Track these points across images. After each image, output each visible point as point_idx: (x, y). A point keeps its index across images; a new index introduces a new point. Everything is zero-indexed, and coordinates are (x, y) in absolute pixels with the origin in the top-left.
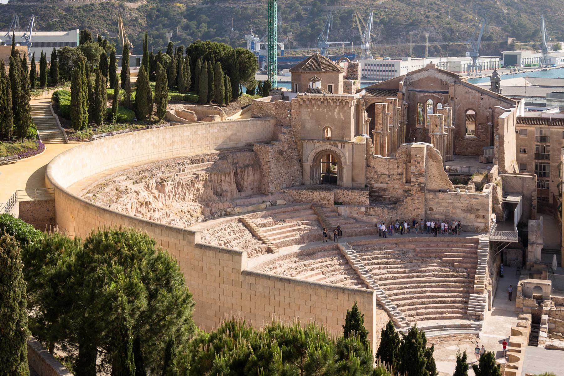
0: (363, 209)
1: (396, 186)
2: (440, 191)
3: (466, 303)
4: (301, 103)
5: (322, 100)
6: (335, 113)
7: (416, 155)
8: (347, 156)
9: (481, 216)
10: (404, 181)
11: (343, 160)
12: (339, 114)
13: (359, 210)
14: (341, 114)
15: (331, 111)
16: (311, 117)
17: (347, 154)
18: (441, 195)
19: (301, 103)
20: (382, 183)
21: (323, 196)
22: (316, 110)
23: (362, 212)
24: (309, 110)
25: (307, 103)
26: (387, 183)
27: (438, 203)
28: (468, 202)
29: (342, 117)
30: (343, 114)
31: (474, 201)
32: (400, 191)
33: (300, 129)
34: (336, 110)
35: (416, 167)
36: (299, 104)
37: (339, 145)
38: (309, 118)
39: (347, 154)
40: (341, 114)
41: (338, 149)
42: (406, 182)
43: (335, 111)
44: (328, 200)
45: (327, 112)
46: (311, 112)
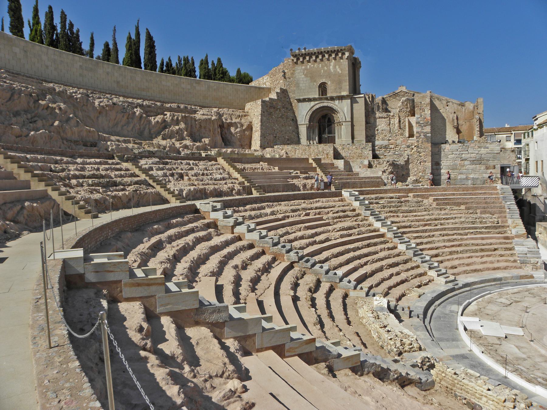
0: (366, 162)
1: (399, 142)
5: (317, 54)
6: (331, 67)
7: (421, 103)
9: (492, 166)
10: (408, 136)
12: (335, 67)
13: (362, 163)
14: (337, 67)
15: (326, 65)
17: (345, 109)
20: (383, 140)
21: (321, 149)
22: (310, 66)
23: (365, 165)
24: (303, 67)
26: (389, 140)
28: (477, 152)
29: (338, 70)
30: (339, 67)
34: (332, 64)
35: (421, 116)
38: (303, 76)
39: (345, 109)
40: (337, 67)
41: (336, 105)
42: (409, 137)
43: (330, 65)
44: (327, 154)
45: (323, 67)
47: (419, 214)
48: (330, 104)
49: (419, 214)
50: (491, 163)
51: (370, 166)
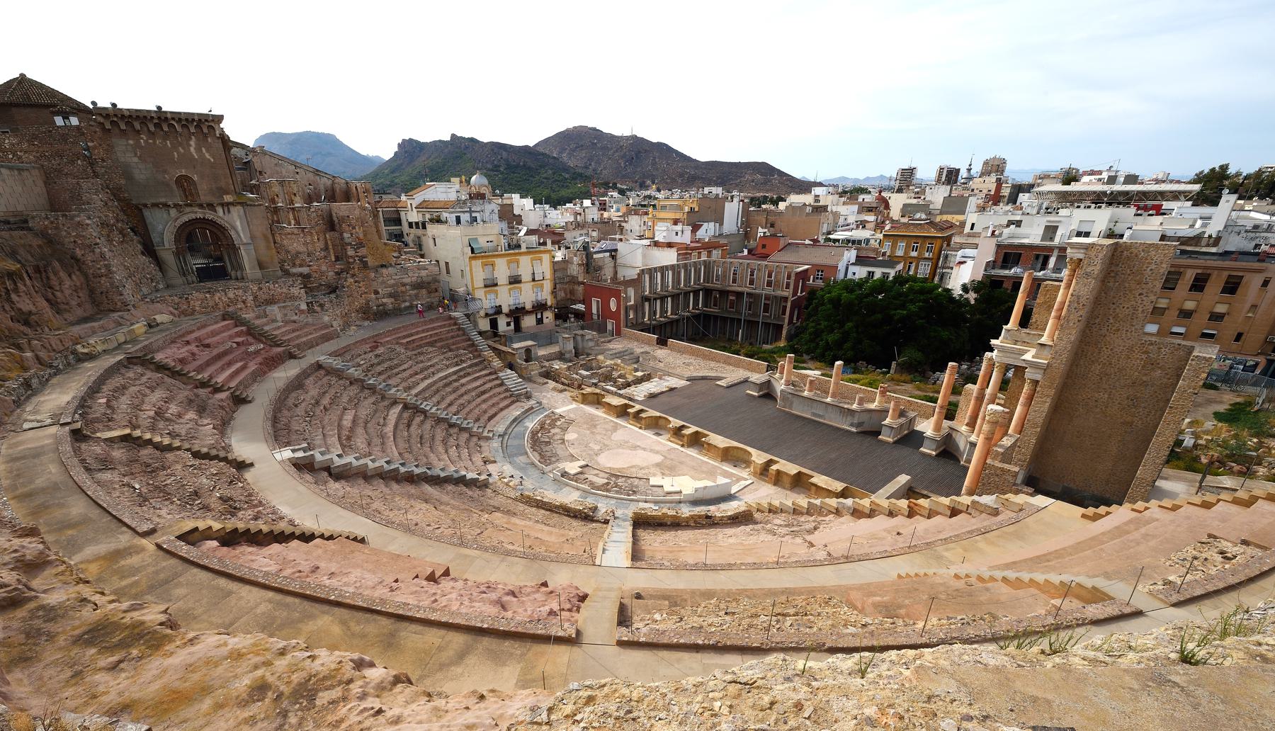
0: (304, 307)
1: (324, 268)
2: (382, 266)
3: (502, 384)
4: (108, 126)
8: (239, 228)
11: (232, 233)
13: (297, 307)
16: (140, 158)
17: (238, 223)
18: (384, 271)
19: (108, 126)
20: (301, 266)
25: (123, 127)
27: (383, 282)
31: (424, 273)
32: (331, 274)
33: (123, 182)
36: (104, 129)
37: (220, 210)
39: (238, 223)
41: (219, 215)
44: (244, 302)
46: (138, 145)
47: (406, 366)
48: (210, 215)
49: (406, 366)
50: (433, 287)
51: (311, 310)
